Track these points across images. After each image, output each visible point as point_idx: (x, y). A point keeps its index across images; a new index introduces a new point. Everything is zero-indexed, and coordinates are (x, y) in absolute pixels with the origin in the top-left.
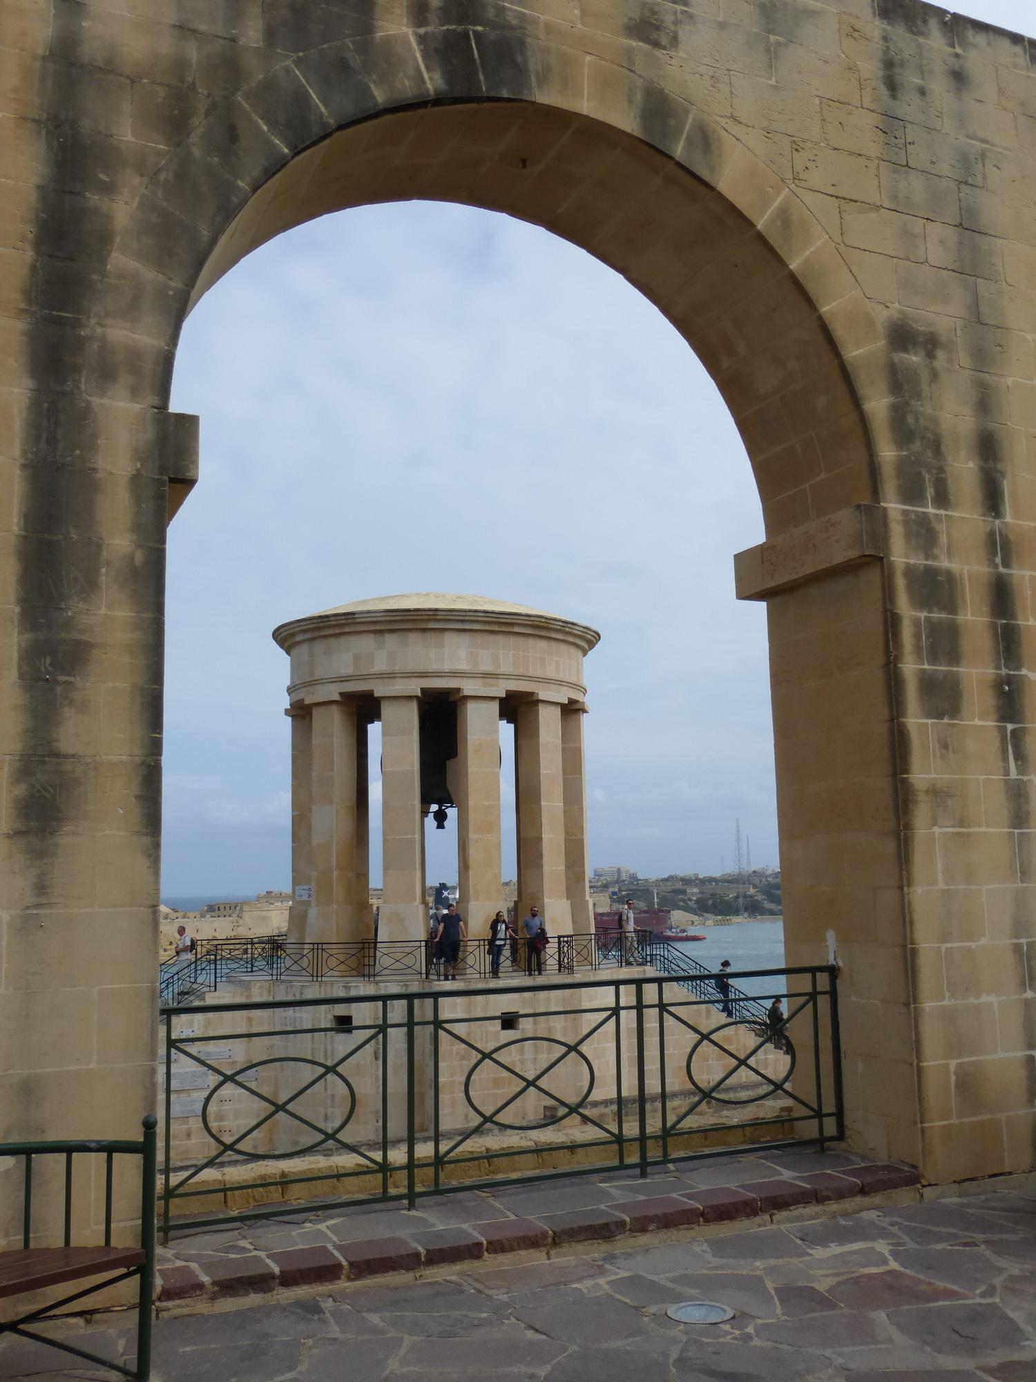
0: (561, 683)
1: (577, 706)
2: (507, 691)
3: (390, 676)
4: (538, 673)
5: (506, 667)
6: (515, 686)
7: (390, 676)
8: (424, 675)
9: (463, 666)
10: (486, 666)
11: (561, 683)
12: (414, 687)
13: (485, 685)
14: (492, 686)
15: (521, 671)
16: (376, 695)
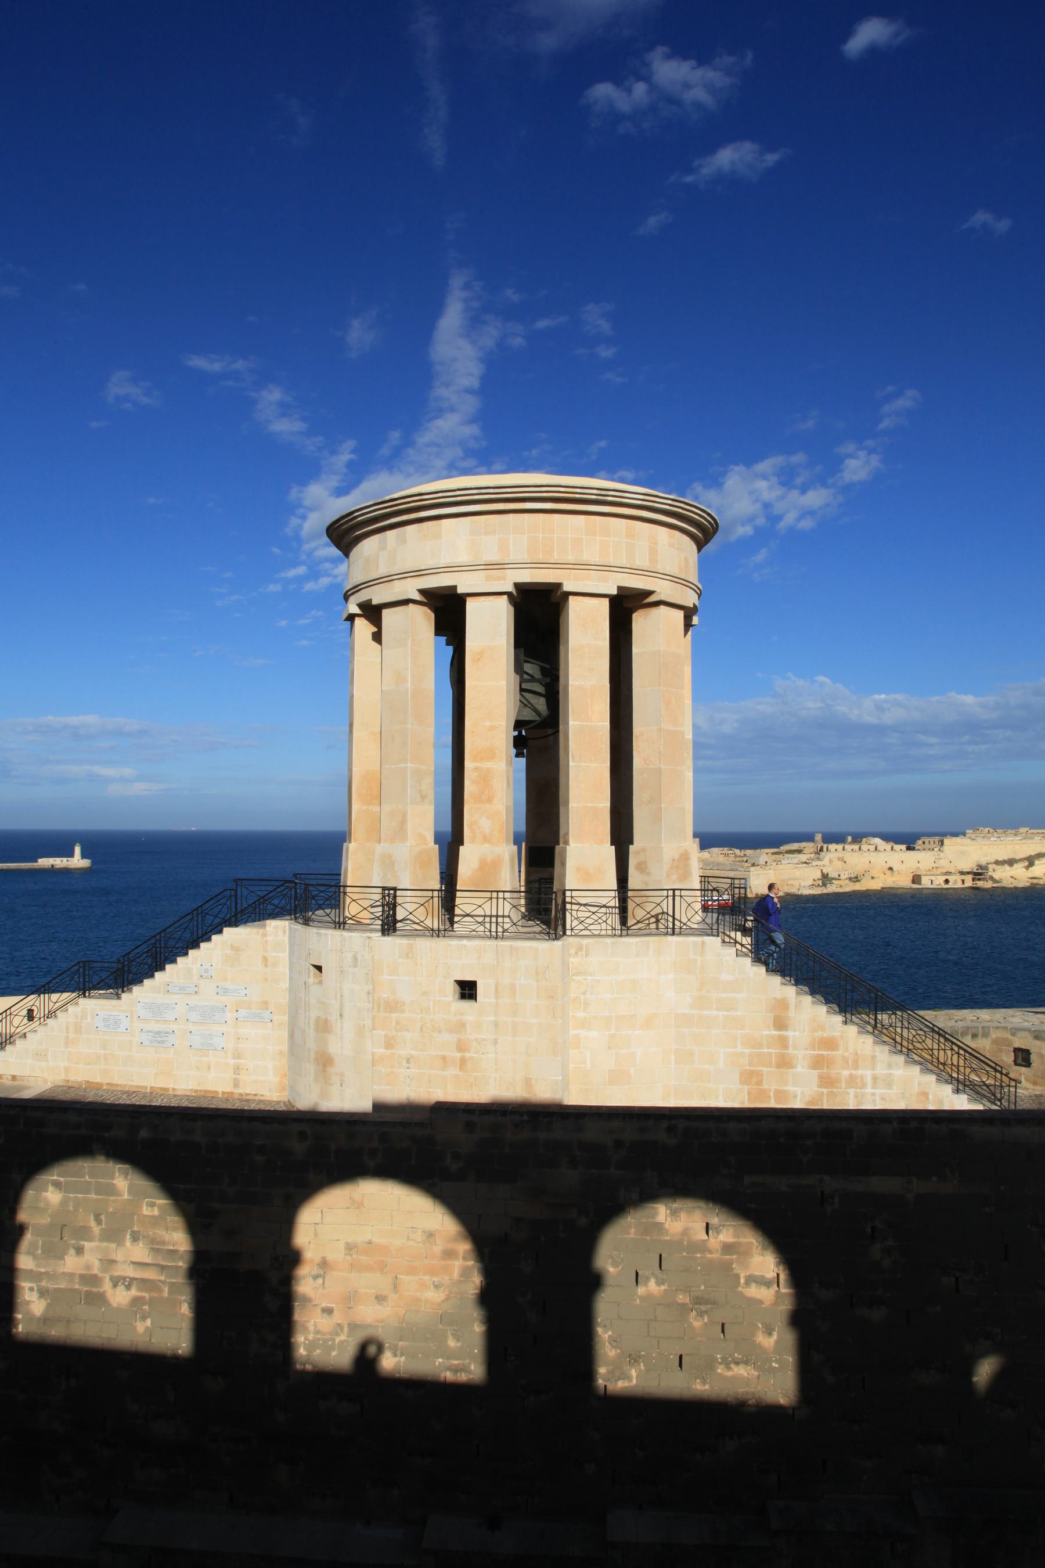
0: (607, 568)
1: (652, 599)
2: (517, 585)
3: (387, 579)
4: (570, 558)
5: (518, 552)
6: (527, 577)
7: (387, 579)
8: (419, 573)
9: (463, 558)
10: (492, 556)
11: (607, 568)
12: (410, 589)
13: (488, 579)
14: (499, 579)
15: (541, 557)
16: (374, 602)
